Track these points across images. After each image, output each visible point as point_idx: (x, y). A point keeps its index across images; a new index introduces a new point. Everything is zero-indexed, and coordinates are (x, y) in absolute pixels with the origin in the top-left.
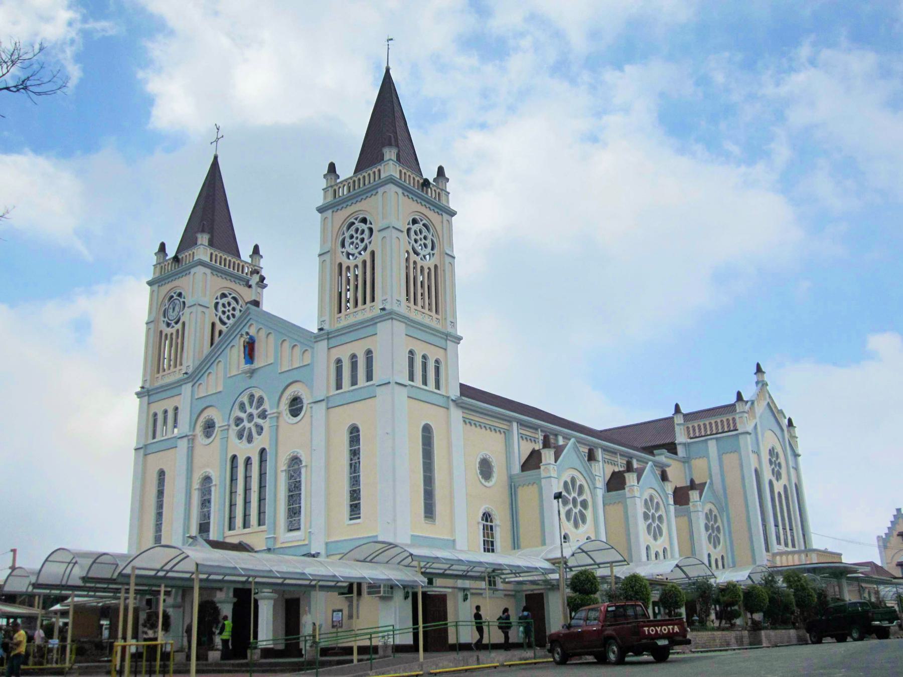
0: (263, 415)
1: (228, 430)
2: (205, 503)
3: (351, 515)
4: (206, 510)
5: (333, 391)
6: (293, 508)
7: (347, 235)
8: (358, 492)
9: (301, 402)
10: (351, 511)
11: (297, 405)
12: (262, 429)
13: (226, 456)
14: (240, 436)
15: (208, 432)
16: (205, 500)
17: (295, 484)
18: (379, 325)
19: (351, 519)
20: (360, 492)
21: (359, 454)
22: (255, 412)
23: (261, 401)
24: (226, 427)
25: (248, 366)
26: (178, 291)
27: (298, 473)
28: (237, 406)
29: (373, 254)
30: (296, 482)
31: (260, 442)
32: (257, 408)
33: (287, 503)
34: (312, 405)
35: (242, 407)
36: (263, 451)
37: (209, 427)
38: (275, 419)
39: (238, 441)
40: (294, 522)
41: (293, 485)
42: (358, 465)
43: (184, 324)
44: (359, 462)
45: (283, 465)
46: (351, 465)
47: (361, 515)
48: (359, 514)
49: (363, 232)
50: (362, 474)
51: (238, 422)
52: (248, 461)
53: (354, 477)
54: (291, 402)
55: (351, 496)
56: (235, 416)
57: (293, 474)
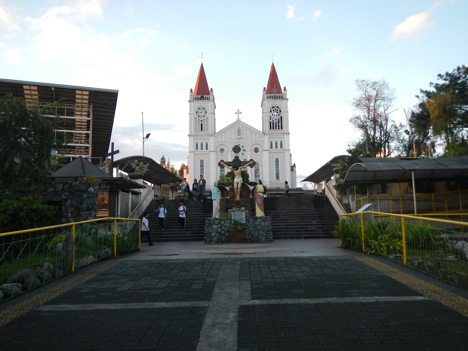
0: (245, 150)
4: (222, 172)
7: (272, 110)
9: (258, 149)
25: (239, 137)
29: (281, 117)
46: (276, 167)
49: (277, 110)
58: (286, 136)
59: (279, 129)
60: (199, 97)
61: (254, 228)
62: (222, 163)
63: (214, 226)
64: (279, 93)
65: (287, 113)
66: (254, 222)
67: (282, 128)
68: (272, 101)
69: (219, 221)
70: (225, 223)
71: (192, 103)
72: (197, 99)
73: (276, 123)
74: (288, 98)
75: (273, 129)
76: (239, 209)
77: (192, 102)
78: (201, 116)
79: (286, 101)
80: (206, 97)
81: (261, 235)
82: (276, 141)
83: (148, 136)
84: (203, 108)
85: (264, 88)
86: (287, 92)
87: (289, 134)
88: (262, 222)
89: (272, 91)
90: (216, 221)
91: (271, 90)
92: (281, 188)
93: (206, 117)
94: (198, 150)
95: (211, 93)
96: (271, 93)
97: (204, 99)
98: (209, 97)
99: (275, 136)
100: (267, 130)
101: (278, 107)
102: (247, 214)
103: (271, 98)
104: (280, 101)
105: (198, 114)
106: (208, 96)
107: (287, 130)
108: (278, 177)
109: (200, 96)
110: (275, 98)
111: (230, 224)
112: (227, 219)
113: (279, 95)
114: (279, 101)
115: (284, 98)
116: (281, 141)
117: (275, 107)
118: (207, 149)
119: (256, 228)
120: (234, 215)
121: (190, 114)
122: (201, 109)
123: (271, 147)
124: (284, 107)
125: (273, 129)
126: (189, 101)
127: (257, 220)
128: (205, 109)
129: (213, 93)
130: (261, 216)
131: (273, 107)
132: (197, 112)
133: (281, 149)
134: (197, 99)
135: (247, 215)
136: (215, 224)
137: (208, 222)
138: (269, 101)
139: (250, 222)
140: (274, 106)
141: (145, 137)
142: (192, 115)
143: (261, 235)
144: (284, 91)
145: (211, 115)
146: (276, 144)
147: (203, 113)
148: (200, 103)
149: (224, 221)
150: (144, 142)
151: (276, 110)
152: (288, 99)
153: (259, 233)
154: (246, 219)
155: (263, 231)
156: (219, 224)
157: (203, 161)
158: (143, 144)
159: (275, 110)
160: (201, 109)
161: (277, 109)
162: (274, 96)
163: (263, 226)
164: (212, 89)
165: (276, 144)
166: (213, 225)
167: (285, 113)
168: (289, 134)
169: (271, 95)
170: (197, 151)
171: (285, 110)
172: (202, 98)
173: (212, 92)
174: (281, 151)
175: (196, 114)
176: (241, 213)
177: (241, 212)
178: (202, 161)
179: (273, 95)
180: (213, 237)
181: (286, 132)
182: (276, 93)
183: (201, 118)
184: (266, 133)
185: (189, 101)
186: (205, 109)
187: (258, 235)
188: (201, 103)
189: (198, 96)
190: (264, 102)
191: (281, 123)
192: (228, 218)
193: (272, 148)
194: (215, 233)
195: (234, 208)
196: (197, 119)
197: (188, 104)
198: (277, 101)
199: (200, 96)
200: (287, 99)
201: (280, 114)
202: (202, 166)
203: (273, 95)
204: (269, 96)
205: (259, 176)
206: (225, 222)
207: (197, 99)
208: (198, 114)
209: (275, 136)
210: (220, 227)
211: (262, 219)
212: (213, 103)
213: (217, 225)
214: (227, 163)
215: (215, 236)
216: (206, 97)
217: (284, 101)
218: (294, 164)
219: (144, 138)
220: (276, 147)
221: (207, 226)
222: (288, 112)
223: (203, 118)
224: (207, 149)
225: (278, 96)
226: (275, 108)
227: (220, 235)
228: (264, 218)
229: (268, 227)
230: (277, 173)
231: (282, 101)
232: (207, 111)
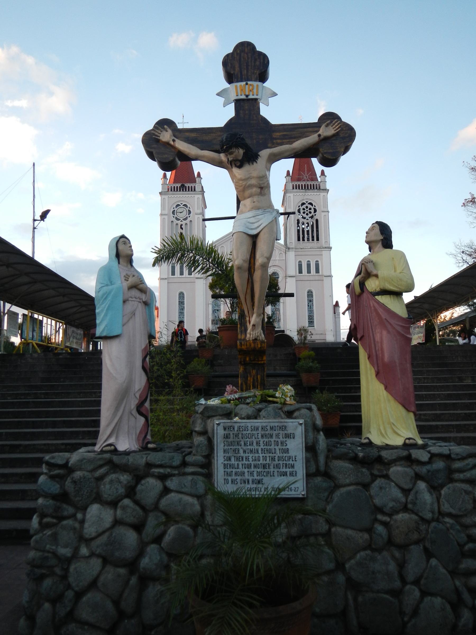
4: (216, 314)
7: (301, 208)
10: (309, 324)
21: (313, 302)
29: (317, 221)
42: (312, 306)
44: (313, 305)
46: (308, 305)
58: (324, 253)
59: (313, 240)
60: (177, 187)
61: (370, 530)
62: (166, 136)
63: (94, 509)
64: (312, 180)
65: (327, 213)
66: (366, 486)
67: (318, 239)
68: (301, 194)
69: (125, 478)
70: (166, 491)
71: (166, 197)
72: (174, 189)
73: (308, 231)
74: (328, 188)
75: (303, 240)
76: (258, 393)
77: (165, 194)
78: (181, 219)
79: (325, 194)
80: (189, 187)
81: (416, 582)
82: (309, 261)
83: (44, 216)
84: (185, 205)
85: (288, 172)
86: (327, 179)
87: (331, 248)
88: (422, 485)
89: (301, 177)
90: (107, 479)
91: (299, 175)
92: (317, 341)
93: (189, 219)
94: (176, 276)
95: (197, 179)
96: (299, 180)
97: (186, 190)
98: (195, 187)
99: (307, 253)
100: (293, 242)
101: (311, 204)
102: (316, 429)
103: (299, 188)
104: (315, 194)
105: (176, 216)
106: (193, 185)
107: (328, 241)
108: (311, 322)
109: (179, 185)
110: (307, 188)
111: (198, 497)
112: (184, 464)
113: (312, 183)
114: (312, 194)
115: (321, 188)
116: (317, 261)
117: (307, 204)
119: (380, 529)
120: (226, 437)
121: (161, 215)
122: (182, 206)
123: (300, 272)
124: (322, 204)
125: (303, 240)
126: (160, 193)
127: (386, 477)
128: (187, 207)
129: (200, 181)
130: (399, 442)
131: (303, 204)
132: (173, 212)
133: (317, 274)
134: (174, 190)
135: (316, 442)
136: (98, 499)
137: (55, 488)
138: (295, 194)
139: (337, 487)
140: (304, 202)
141: (38, 217)
142: (166, 217)
143: (416, 582)
144: (322, 177)
145: (196, 216)
146: (309, 266)
147: (185, 212)
148: (178, 196)
149: (163, 478)
150: (34, 228)
151: (308, 209)
152: (328, 190)
153: (401, 565)
154: (313, 469)
155: (429, 554)
156: (127, 501)
157: (183, 294)
158: (34, 232)
160: (182, 206)
161: (310, 206)
162: (305, 185)
163: (428, 516)
164: (199, 174)
165: (309, 266)
166: (84, 509)
167: (323, 214)
168: (331, 248)
169: (300, 183)
170: (172, 276)
171: (323, 209)
172: (183, 188)
173: (199, 179)
174: (317, 278)
175: (172, 215)
176: (275, 422)
177: (276, 416)
178: (181, 295)
179: (303, 183)
180: (79, 595)
181: (324, 246)
182: (308, 181)
183: (181, 221)
184: (291, 247)
185: (160, 193)
186: (187, 207)
187: (397, 584)
188: (181, 196)
189: (176, 185)
190: (288, 195)
191: (317, 231)
192: (189, 459)
193: (302, 273)
194: (96, 563)
195: (229, 388)
196: (175, 223)
197: (159, 198)
198: (309, 194)
199: (179, 185)
200: (327, 191)
201: (315, 215)
202: (181, 303)
203: (303, 183)
204: (296, 185)
206: (172, 483)
207: (174, 190)
208: (176, 216)
209: (307, 253)
210: (131, 520)
211: (423, 470)
212: (200, 196)
213: (114, 504)
214: (193, 135)
215: (93, 584)
216: (189, 187)
217: (322, 194)
218: (337, 302)
219: (35, 220)
220: (309, 271)
221: (42, 516)
222: (328, 212)
223: (184, 222)
225: (311, 185)
226: (307, 205)
227: (134, 580)
228: (430, 462)
229: (466, 527)
230: (311, 316)
231: (318, 194)
232: (191, 210)
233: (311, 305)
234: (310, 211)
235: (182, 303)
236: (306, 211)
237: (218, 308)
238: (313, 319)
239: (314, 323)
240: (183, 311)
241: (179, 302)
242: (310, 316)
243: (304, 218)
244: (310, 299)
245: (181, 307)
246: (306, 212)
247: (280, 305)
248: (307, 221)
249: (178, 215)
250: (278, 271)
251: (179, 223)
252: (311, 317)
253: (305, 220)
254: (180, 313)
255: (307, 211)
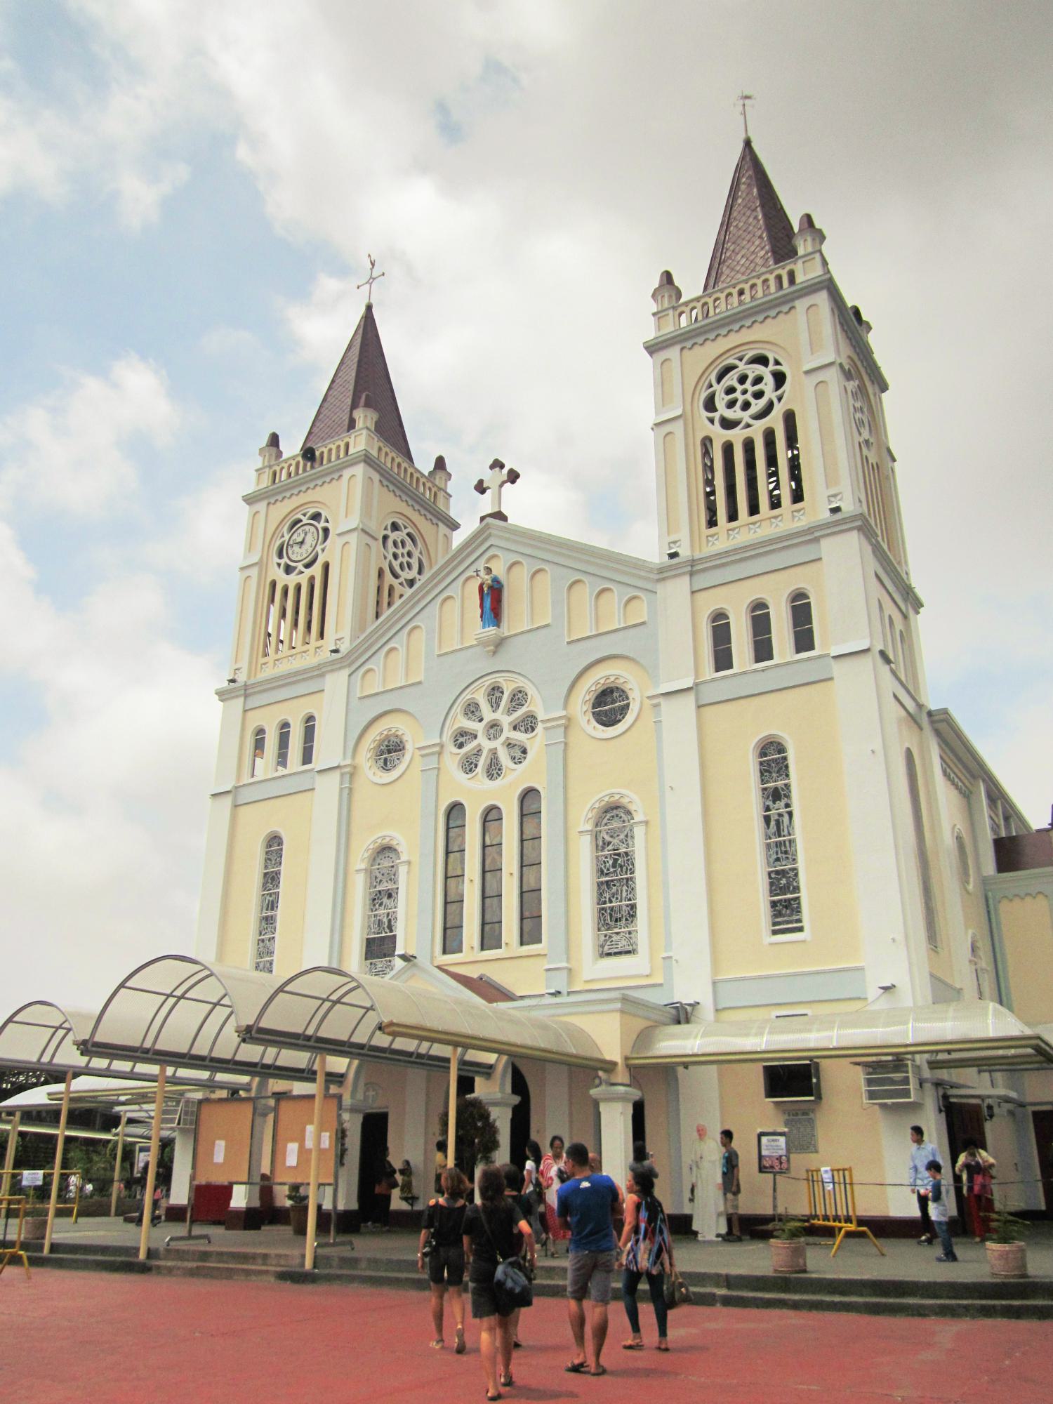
0: (528, 724)
1: (440, 754)
2: (382, 896)
3: (774, 924)
4: (382, 911)
5: (708, 671)
6: (612, 909)
8: (791, 874)
9: (624, 694)
10: (775, 916)
11: (614, 702)
12: (524, 752)
13: (437, 806)
14: (469, 766)
15: (386, 760)
16: (380, 892)
17: (616, 860)
18: (824, 542)
19: (775, 933)
20: (796, 875)
21: (788, 796)
22: (506, 721)
23: (518, 698)
24: (437, 749)
26: (311, 511)
27: (622, 836)
28: (458, 708)
29: (790, 418)
30: (619, 855)
31: (515, 779)
32: (510, 711)
33: (595, 901)
34: (661, 700)
35: (472, 710)
36: (529, 795)
37: (390, 751)
38: (562, 729)
39: (462, 777)
40: (615, 938)
41: (611, 862)
43: (326, 567)
44: (790, 814)
45: (583, 820)
46: (767, 819)
47: (806, 923)
48: (799, 921)
50: (798, 834)
51: (461, 740)
52: (491, 816)
53: (778, 844)
54: (597, 698)
55: (771, 884)
56: (456, 727)
57: (608, 838)
82: (760, 605)
101: (762, 360)
118: (307, 757)
123: (723, 660)
146: (761, 624)
151: (748, 385)
159: (740, 388)
165: (761, 624)
202: (271, 879)
205: (632, 915)
223: (308, 572)
224: (307, 757)
230: (782, 873)
233: (780, 815)
234: (757, 387)
235: (273, 879)
236: (737, 395)
237: (390, 886)
238: (797, 889)
239: (798, 910)
240: (273, 913)
241: (266, 874)
242: (777, 872)
243: (728, 424)
244: (772, 785)
245: (268, 898)
246: (741, 399)
247: (633, 837)
248: (747, 433)
249: (293, 553)
250: (622, 680)
251: (292, 580)
252: (784, 881)
253: (737, 431)
254: (264, 924)
255: (745, 392)
